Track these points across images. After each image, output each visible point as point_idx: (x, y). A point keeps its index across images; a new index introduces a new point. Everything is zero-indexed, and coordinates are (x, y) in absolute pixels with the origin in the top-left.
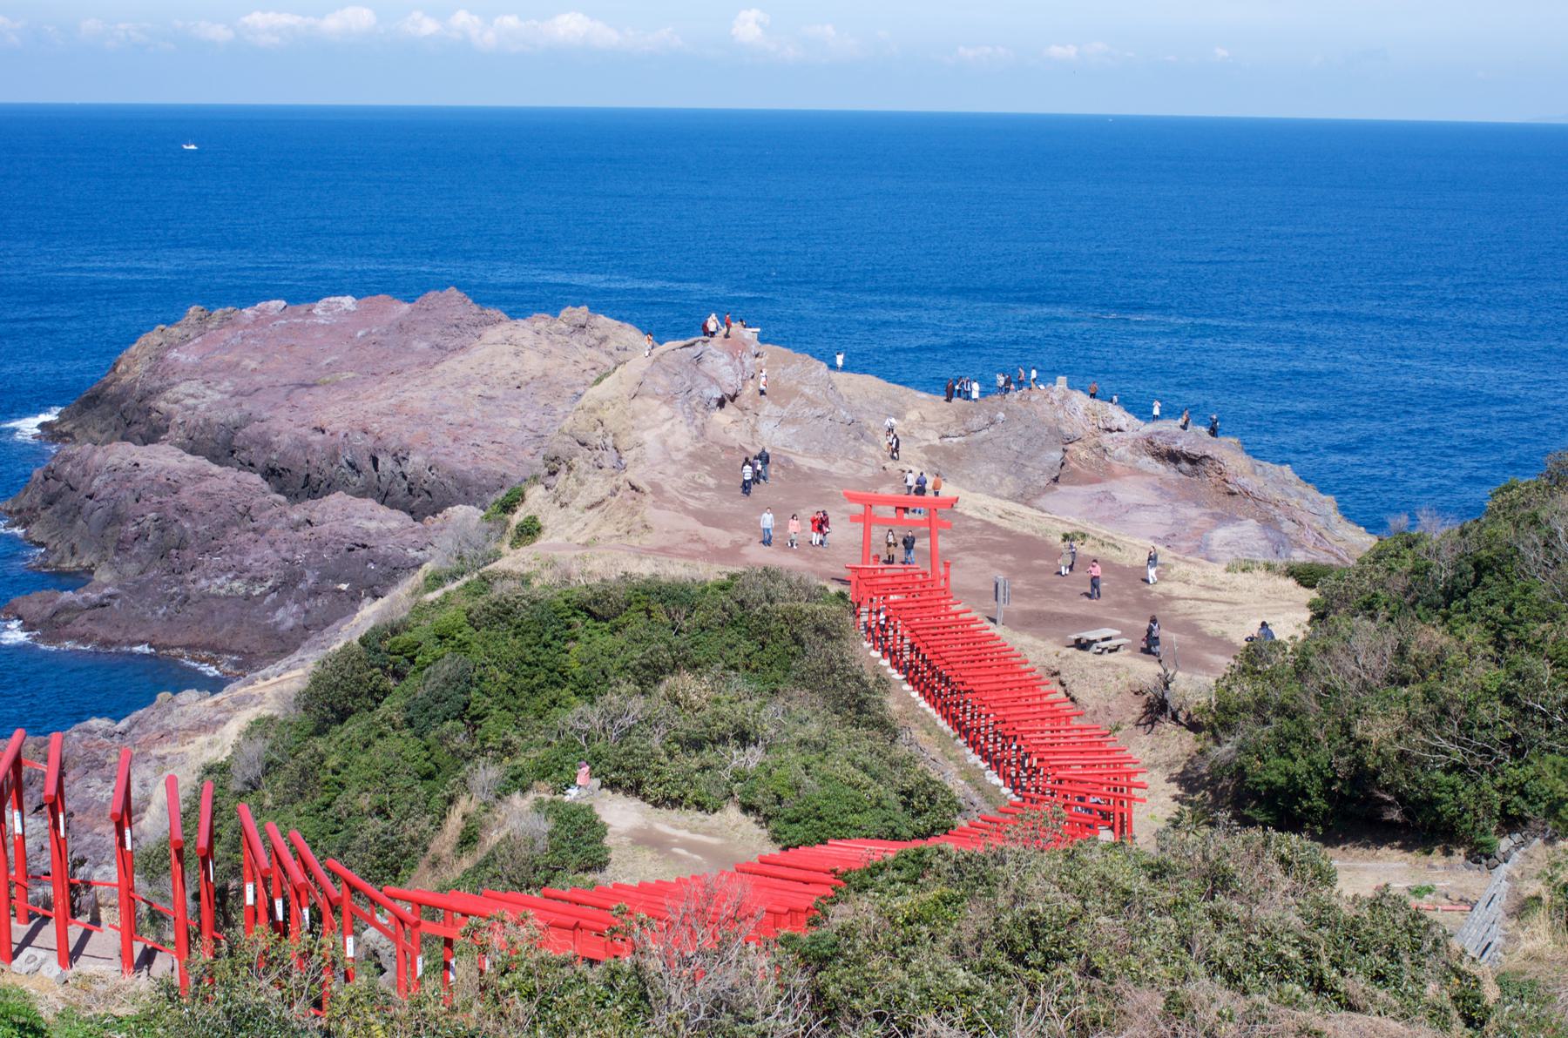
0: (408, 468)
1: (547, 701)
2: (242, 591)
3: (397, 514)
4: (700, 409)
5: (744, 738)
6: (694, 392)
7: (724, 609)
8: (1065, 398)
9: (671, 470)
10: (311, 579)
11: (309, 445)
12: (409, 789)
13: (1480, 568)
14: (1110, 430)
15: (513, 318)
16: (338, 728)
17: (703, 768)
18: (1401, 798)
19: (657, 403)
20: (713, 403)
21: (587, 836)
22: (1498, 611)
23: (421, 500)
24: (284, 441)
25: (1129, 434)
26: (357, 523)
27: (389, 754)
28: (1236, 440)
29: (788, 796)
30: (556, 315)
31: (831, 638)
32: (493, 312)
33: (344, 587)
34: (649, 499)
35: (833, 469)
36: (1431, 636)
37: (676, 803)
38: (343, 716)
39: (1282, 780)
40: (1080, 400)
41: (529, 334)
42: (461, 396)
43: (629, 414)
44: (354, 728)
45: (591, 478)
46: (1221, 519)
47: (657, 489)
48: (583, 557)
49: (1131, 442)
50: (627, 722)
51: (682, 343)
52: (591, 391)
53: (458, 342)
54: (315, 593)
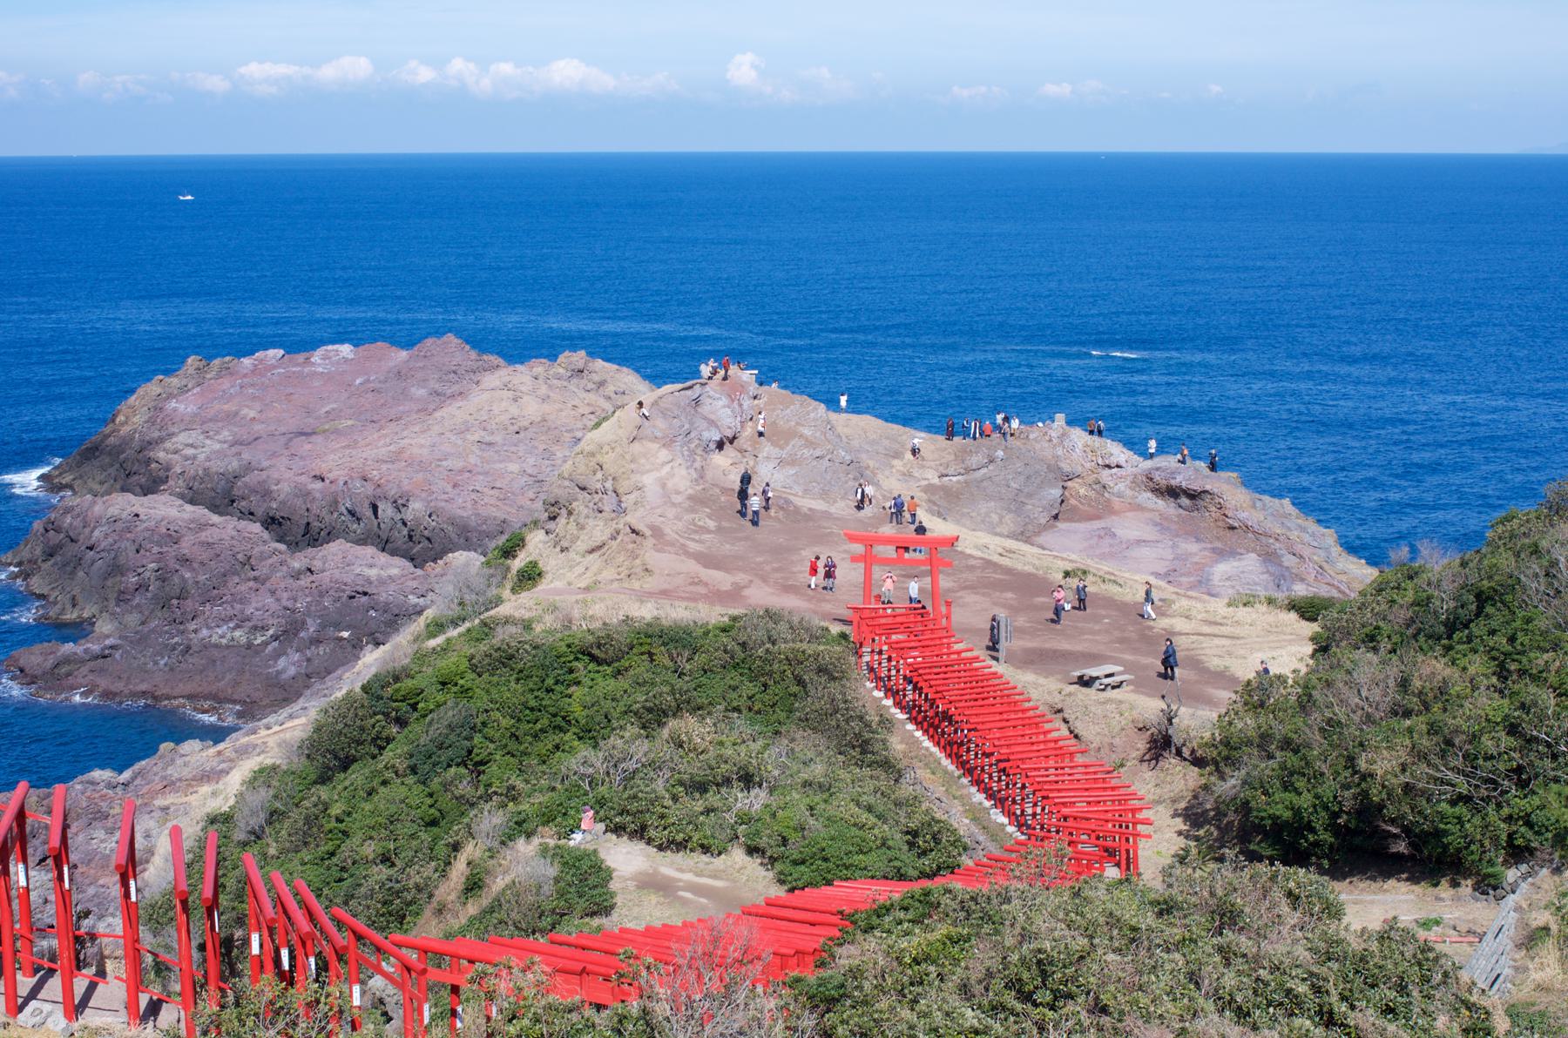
0: (408, 515)
1: (550, 746)
2: (244, 640)
3: (398, 561)
4: (699, 451)
5: (748, 780)
7: (725, 651)
9: (671, 513)
10: (312, 627)
11: (309, 493)
12: (413, 836)
13: (1482, 599)
14: (1109, 467)
17: (708, 811)
18: (1407, 830)
21: (592, 881)
22: (1501, 641)
23: (421, 546)
25: (1129, 470)
26: (358, 571)
27: (393, 802)
28: (1235, 475)
29: (793, 837)
30: (553, 357)
31: (834, 679)
33: (345, 634)
34: (650, 542)
35: (833, 510)
36: (1432, 668)
38: (346, 764)
39: (1287, 814)
40: (1079, 436)
41: (527, 379)
42: (459, 442)
43: (628, 457)
44: (357, 776)
45: (591, 522)
46: (1221, 554)
47: (657, 532)
48: (585, 602)
50: (631, 765)
51: (680, 386)
53: (456, 388)
54: (316, 641)
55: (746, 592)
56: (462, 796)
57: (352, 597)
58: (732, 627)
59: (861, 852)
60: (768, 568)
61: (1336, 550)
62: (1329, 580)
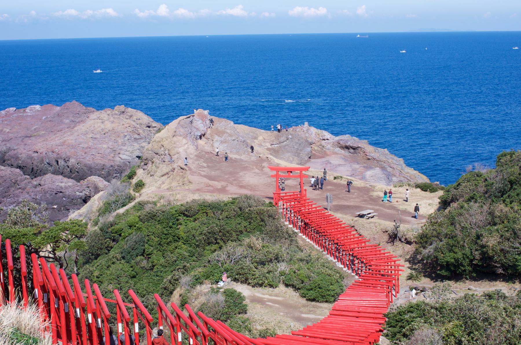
0: (70, 164)
1: (174, 247)
3: (70, 180)
6: (192, 134)
8: (308, 129)
11: (32, 157)
12: (127, 282)
13: (512, 183)
14: (324, 140)
15: (98, 110)
16: (95, 261)
17: (269, 272)
19: (181, 138)
20: (198, 137)
21: (239, 301)
23: (78, 174)
24: (23, 156)
25: (331, 141)
26: (57, 184)
28: (366, 141)
29: (306, 280)
31: (274, 219)
33: (55, 207)
34: (188, 172)
37: (261, 285)
38: (97, 256)
39: (453, 260)
40: (313, 130)
41: (106, 115)
44: (102, 261)
45: (161, 165)
46: (368, 168)
47: (190, 169)
49: (332, 143)
51: (186, 117)
52: (157, 135)
55: (227, 189)
56: (144, 267)
59: (331, 284)
60: (231, 180)
62: (404, 175)
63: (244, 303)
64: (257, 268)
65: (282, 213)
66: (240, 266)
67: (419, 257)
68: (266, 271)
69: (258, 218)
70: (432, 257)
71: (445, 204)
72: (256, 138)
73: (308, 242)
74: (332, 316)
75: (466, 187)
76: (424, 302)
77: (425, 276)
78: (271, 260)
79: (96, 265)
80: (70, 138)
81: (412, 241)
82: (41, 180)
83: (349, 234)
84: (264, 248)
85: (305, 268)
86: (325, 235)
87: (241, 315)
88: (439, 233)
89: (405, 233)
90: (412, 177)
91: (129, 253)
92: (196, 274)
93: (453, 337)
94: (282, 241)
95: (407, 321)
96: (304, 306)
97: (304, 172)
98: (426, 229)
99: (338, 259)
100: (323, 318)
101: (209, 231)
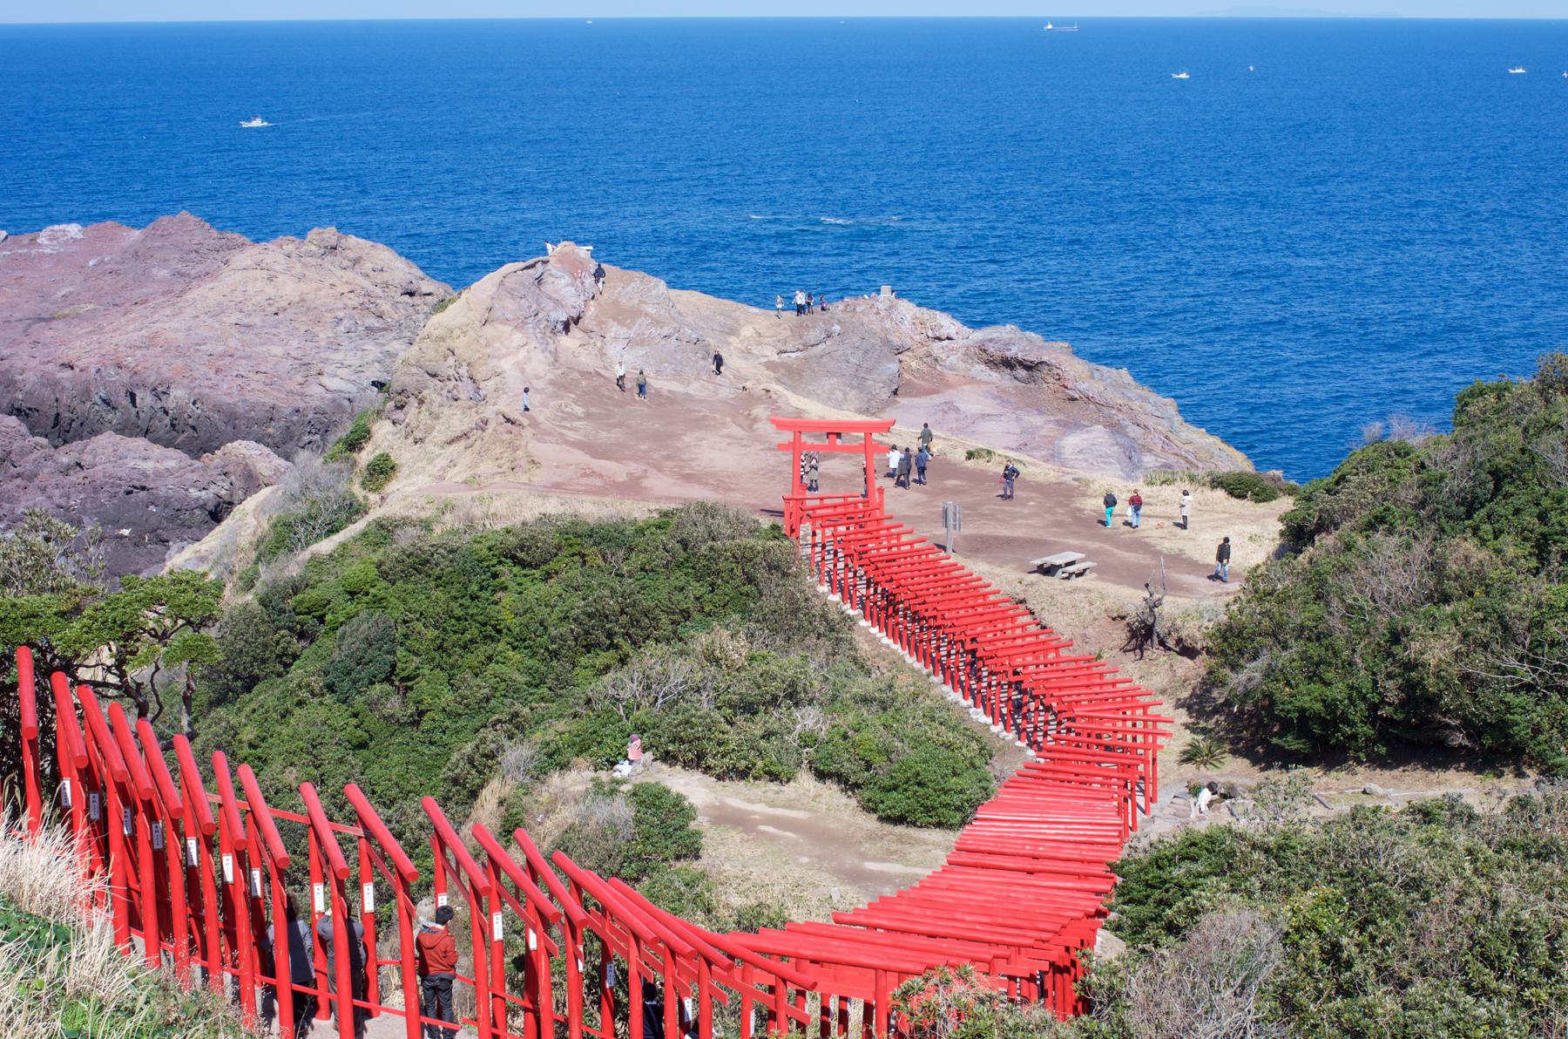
0: (170, 403)
1: (482, 658)
3: (171, 452)
5: (794, 695)
6: (540, 316)
8: (891, 307)
11: (57, 383)
12: (341, 761)
13: (1498, 476)
14: (939, 339)
15: (257, 241)
16: (246, 697)
17: (767, 736)
18: (1468, 725)
19: (508, 329)
23: (195, 435)
24: (30, 378)
25: (959, 342)
28: (1066, 345)
29: (879, 760)
30: (301, 234)
31: (785, 575)
32: (236, 235)
33: (126, 532)
36: (1465, 551)
37: (743, 774)
38: (250, 683)
39: (1318, 706)
40: (907, 308)
41: (281, 258)
44: (266, 696)
47: (534, 424)
49: (962, 350)
51: (521, 265)
52: (436, 318)
53: (200, 268)
55: (645, 483)
56: (392, 716)
57: (129, 493)
58: (668, 524)
59: (955, 774)
60: (656, 456)
61: (1178, 419)
62: (1176, 450)
63: (693, 825)
64: (731, 724)
65: (810, 558)
66: (680, 717)
67: (1219, 695)
68: (759, 733)
69: (738, 572)
70: (1258, 695)
71: (1298, 535)
72: (733, 332)
73: (888, 646)
74: (956, 868)
75: (1361, 486)
76: (1230, 831)
77: (1234, 752)
78: (775, 698)
79: (248, 709)
80: (172, 324)
81: (1199, 646)
82: (82, 452)
83: (1009, 625)
84: (755, 664)
85: (878, 723)
86: (938, 627)
87: (682, 864)
88: (1280, 626)
89: (1179, 622)
90: (1202, 455)
91: (349, 673)
92: (548, 738)
93: (1314, 935)
94: (807, 642)
95: (1180, 886)
96: (872, 837)
97: (876, 436)
98: (1241, 612)
99: (974, 698)
100: (929, 872)
101: (589, 610)
